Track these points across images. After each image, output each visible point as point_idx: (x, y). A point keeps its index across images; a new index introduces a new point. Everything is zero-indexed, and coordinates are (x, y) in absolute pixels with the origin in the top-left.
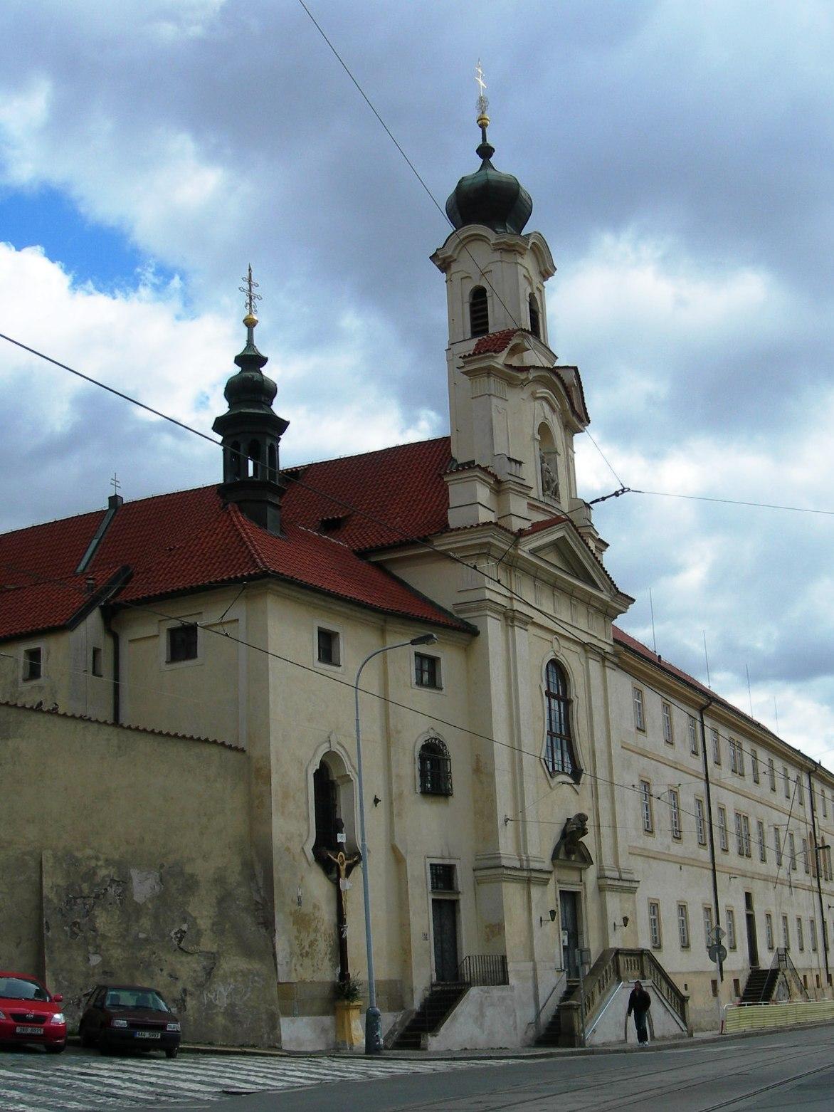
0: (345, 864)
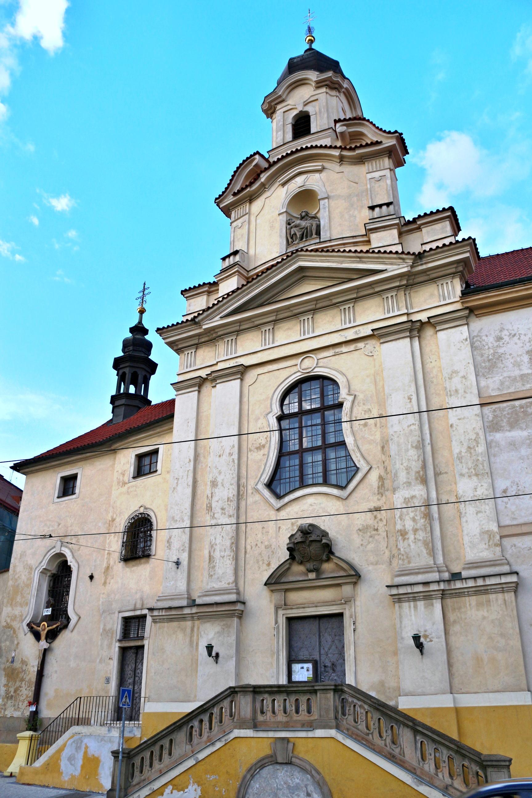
0: (46, 631)
